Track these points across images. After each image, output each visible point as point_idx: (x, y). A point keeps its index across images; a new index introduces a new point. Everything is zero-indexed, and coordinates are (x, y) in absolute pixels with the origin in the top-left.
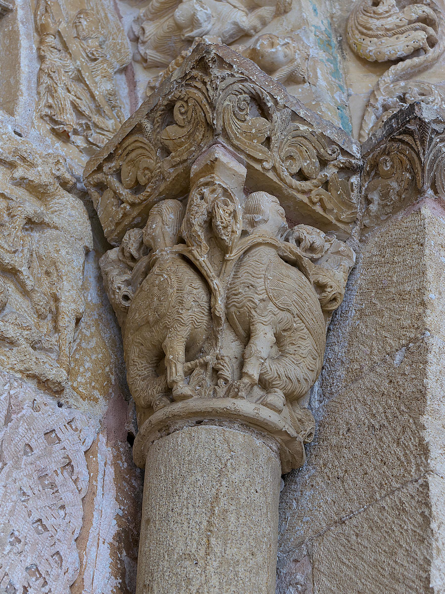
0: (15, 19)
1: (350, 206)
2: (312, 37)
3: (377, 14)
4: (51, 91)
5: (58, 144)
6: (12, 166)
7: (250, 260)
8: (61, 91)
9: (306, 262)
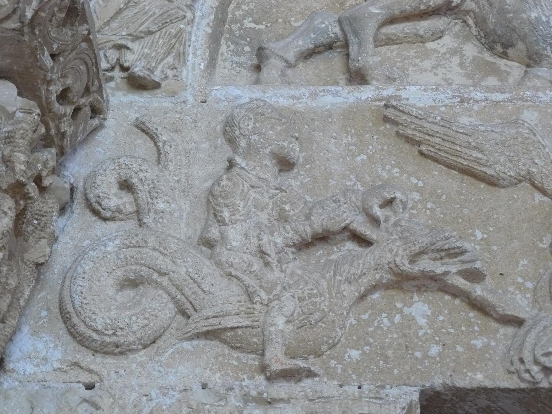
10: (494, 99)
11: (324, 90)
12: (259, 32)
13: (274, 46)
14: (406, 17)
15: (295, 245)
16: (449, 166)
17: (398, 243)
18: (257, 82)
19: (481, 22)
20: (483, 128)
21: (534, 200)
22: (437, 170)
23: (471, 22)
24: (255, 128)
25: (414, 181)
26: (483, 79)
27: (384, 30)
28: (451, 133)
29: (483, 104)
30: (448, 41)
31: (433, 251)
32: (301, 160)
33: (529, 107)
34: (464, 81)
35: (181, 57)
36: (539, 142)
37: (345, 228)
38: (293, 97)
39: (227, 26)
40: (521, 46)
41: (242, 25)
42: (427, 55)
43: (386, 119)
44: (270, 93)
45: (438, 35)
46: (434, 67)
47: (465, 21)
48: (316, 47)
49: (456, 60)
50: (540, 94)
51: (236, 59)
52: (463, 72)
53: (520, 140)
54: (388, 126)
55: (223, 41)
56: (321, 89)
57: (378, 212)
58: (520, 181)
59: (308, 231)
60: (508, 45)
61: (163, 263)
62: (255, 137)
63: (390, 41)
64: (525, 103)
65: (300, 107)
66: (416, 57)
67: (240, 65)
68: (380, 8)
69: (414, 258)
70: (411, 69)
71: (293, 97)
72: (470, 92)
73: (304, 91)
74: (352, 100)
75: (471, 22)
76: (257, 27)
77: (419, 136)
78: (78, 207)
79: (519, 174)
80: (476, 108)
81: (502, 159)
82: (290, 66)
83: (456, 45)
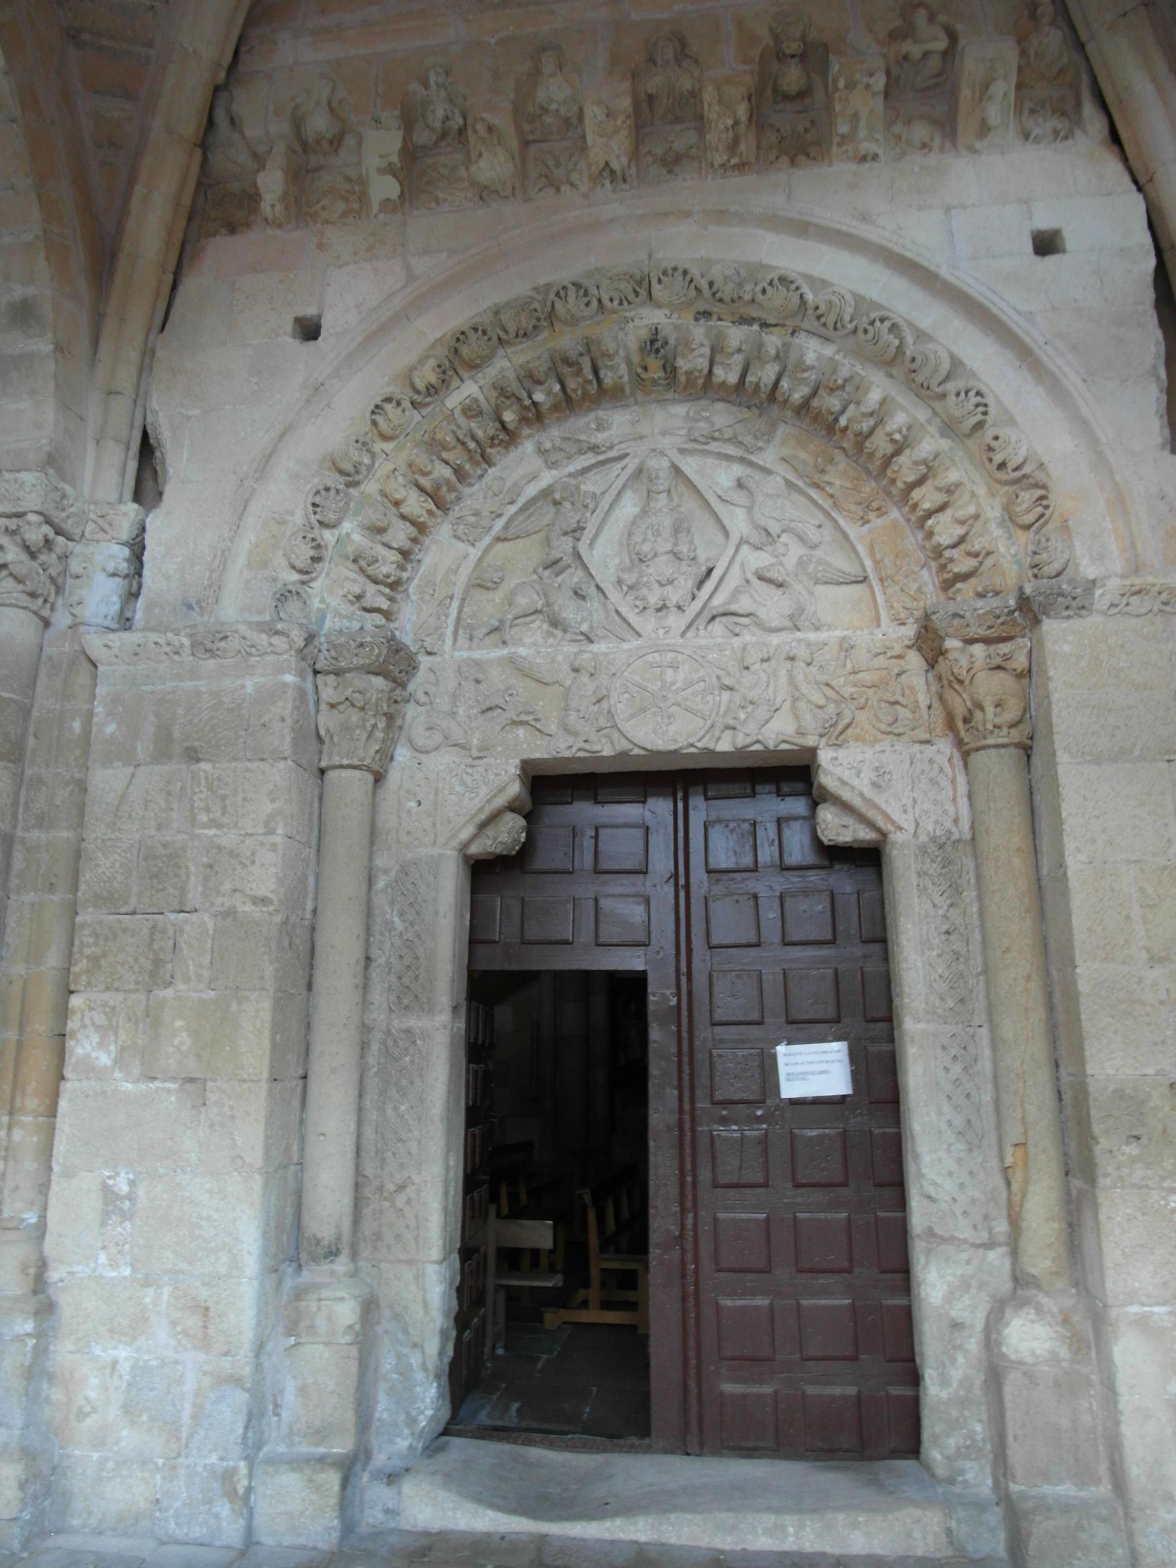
1: (1019, 625)
2: (994, 525)
3: (1019, 505)
4: (892, 607)
5: (902, 628)
6: (885, 653)
7: (975, 679)
8: (896, 605)
9: (1002, 664)
13: (475, 633)
18: (470, 648)
22: (528, 680)
30: (538, 623)
35: (444, 641)
45: (534, 622)
59: (484, 707)
61: (439, 722)
63: (517, 625)
69: (518, 715)
73: (485, 652)
78: (412, 701)
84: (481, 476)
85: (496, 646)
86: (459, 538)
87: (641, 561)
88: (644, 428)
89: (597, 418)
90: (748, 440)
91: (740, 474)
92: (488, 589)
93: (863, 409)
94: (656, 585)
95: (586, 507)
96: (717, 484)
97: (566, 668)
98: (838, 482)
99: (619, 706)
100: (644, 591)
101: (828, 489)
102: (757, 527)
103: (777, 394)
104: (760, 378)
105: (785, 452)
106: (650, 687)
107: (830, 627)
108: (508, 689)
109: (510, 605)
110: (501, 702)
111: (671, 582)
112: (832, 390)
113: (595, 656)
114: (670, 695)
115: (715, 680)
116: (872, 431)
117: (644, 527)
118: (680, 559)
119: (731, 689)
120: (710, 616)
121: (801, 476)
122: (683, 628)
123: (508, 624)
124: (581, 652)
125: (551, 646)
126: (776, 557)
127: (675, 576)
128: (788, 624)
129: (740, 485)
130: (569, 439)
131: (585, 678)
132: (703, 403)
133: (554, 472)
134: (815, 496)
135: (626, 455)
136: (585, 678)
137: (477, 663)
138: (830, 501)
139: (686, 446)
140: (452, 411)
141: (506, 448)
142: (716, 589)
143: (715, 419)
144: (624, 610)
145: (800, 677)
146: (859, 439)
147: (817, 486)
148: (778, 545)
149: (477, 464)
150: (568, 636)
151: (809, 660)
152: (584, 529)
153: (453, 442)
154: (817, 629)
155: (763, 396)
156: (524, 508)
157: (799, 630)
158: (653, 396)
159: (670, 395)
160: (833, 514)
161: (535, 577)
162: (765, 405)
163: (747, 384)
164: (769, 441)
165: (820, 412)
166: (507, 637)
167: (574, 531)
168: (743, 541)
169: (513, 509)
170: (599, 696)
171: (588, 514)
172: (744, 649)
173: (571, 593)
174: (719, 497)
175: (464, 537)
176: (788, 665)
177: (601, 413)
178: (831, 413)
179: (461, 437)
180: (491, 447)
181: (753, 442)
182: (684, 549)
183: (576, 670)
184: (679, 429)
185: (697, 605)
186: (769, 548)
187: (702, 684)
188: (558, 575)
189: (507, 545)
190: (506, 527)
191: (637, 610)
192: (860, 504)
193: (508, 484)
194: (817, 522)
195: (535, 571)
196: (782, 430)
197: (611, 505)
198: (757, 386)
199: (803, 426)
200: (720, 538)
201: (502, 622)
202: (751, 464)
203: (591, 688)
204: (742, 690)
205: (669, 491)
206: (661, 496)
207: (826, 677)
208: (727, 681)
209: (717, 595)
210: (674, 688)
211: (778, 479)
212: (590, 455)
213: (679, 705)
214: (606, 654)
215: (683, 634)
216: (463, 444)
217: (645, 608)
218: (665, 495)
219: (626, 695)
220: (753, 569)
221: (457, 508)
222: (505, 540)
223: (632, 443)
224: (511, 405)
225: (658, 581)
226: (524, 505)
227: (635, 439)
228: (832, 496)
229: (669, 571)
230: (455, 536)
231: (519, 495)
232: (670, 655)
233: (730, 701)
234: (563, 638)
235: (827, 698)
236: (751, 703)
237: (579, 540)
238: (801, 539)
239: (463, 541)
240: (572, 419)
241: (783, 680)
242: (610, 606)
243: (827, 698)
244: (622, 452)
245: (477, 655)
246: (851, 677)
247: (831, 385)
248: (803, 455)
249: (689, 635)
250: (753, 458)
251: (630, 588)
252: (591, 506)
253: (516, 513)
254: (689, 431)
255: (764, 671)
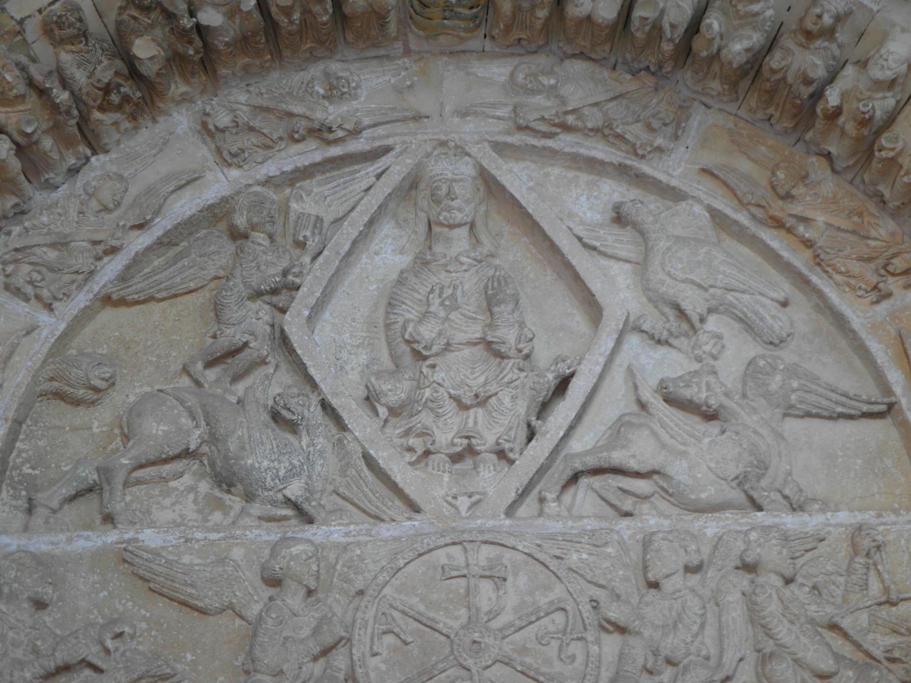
0: (901, 410)
10: (211, 538)
11: (78, 536)
12: (35, 477)
13: (40, 497)
14: (153, 463)
15: (41, 677)
16: (171, 599)
17: (122, 672)
18: (26, 529)
19: (212, 464)
20: (197, 568)
21: (234, 624)
22: (161, 603)
23: (206, 462)
24: (16, 577)
25: (143, 612)
26: (210, 513)
27: (134, 474)
28: (173, 573)
29: (202, 543)
30: (187, 479)
31: (149, 677)
32: (55, 598)
33: (237, 544)
34: (195, 516)
36: (240, 577)
37: (83, 660)
38: (53, 543)
39: (8, 473)
40: (239, 486)
41: (21, 471)
42: (167, 493)
43: (125, 561)
44: (34, 540)
45: (181, 475)
46: (173, 504)
47: (201, 461)
48: (78, 492)
49: (191, 496)
50: (248, 533)
51: (14, 503)
52: (196, 508)
53: (225, 576)
54: (126, 565)
55: (4, 486)
56: (76, 534)
57: (109, 644)
58: (224, 610)
59: (51, 665)
60: (230, 485)
62: (16, 585)
63: (139, 482)
64: (235, 541)
65: (58, 552)
66: (160, 496)
67: (17, 508)
68: (130, 459)
70: (154, 507)
71: (53, 543)
72: (193, 533)
73: (62, 537)
74: (100, 543)
75: (206, 462)
76: (33, 472)
77: (148, 575)
79: (223, 605)
80: (196, 547)
81: (210, 593)
82: (54, 512)
83: (193, 483)
84: (74, 171)
85: (88, 527)
86: (17, 292)
87: (419, 356)
88: (422, 101)
89: (327, 75)
90: (635, 132)
91: (616, 197)
92: (77, 402)
93: (876, 73)
94: (450, 407)
95: (301, 245)
96: (570, 215)
97: (251, 576)
98: (821, 218)
99: (373, 662)
100: (425, 418)
101: (801, 229)
102: (656, 299)
103: (698, 44)
104: (662, 12)
105: (710, 159)
106: (444, 621)
107: (826, 506)
108: (113, 622)
109: (126, 437)
110: (93, 653)
111: (481, 401)
112: (809, 35)
113: (318, 551)
114: (489, 640)
115: (586, 609)
116: (891, 120)
117: (424, 290)
118: (502, 356)
119: (622, 630)
120: (569, 473)
121: (742, 204)
122: (512, 496)
123: (120, 477)
124: (285, 541)
125: (217, 528)
126: (699, 360)
127: (492, 388)
128: (736, 495)
129: (620, 218)
130: (267, 110)
131: (294, 600)
132: (542, 60)
133: (234, 173)
134: (775, 244)
135: (387, 150)
136: (294, 600)
137: (40, 561)
138: (808, 254)
139: (509, 139)
140: (21, 22)
141: (133, 117)
142: (579, 417)
143: (567, 90)
144: (382, 456)
145: (774, 607)
146: (866, 132)
147: (778, 224)
148: (703, 338)
149: (68, 142)
150: (256, 509)
151: (788, 573)
152: (298, 288)
153: (21, 88)
154: (796, 507)
155: (667, 47)
156: (165, 242)
157: (760, 508)
158: (442, 39)
159: (476, 43)
160: (814, 279)
161: (185, 381)
162: (668, 68)
163: (635, 23)
164: (676, 137)
165: (784, 79)
166: (117, 506)
167: (274, 292)
168: (631, 327)
169: (141, 241)
170: (329, 640)
171: (307, 259)
172: (646, 544)
173: (265, 417)
174: (580, 239)
175: (29, 290)
176: (743, 581)
177: (335, 67)
178: (808, 82)
179: (38, 77)
180: (102, 109)
181: (645, 136)
182: (508, 335)
183: (274, 582)
184: (493, 106)
185: (540, 448)
186: (683, 342)
187: (559, 617)
188: (236, 379)
189: (124, 312)
190: (124, 277)
191: (409, 457)
192: (870, 260)
193: (134, 191)
194: (781, 296)
195: (185, 370)
196: (699, 119)
197: (355, 243)
198: (656, 29)
199: (742, 113)
200: (578, 320)
201: (105, 472)
202: (640, 180)
203: (308, 620)
204: (647, 633)
205: (472, 226)
206: (456, 231)
207: (829, 609)
208: (614, 613)
209: (579, 431)
210: (495, 624)
211: (698, 209)
212: (311, 144)
213: (508, 662)
214: (345, 548)
215: (510, 511)
216: (42, 92)
217: (427, 453)
218: (463, 232)
219: (389, 639)
220: (654, 382)
221: (17, 229)
222: (122, 302)
223: (399, 128)
224: (151, 26)
225: (457, 400)
226: (167, 233)
227: (405, 120)
228: (808, 244)
229: (477, 381)
230: (7, 287)
231: (157, 213)
232: (486, 552)
233: (621, 656)
234: (243, 512)
235: (838, 657)
236: (670, 662)
237: (283, 311)
238: (748, 325)
239: (27, 300)
240: (275, 75)
241: (736, 614)
242: (352, 446)
243: (838, 657)
244: (377, 144)
245: (41, 544)
246: (884, 612)
247: (809, 25)
248: (745, 166)
249: (523, 511)
250: (645, 168)
251: (394, 412)
252: (313, 244)
253: (149, 249)
254: (515, 110)
255: (693, 590)
